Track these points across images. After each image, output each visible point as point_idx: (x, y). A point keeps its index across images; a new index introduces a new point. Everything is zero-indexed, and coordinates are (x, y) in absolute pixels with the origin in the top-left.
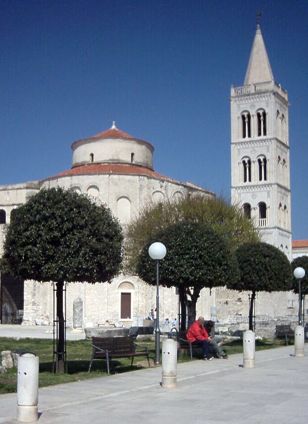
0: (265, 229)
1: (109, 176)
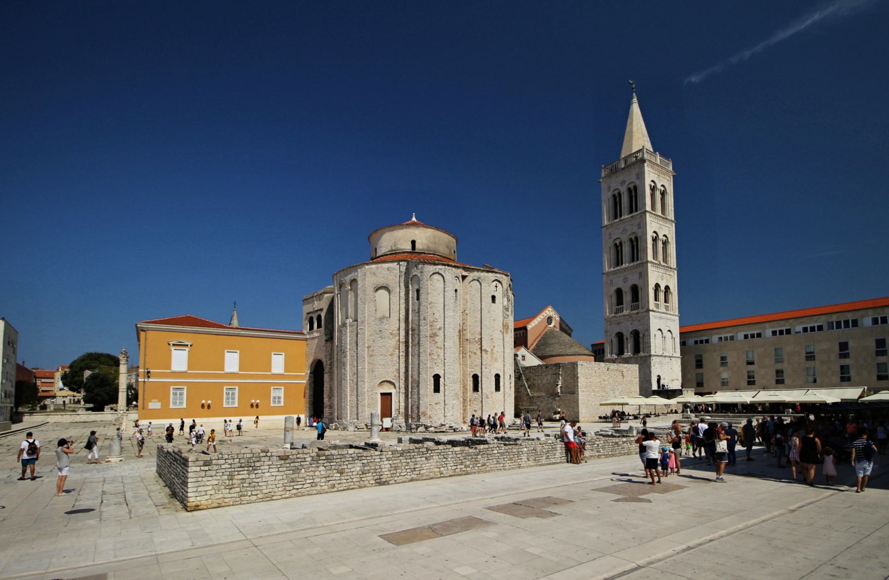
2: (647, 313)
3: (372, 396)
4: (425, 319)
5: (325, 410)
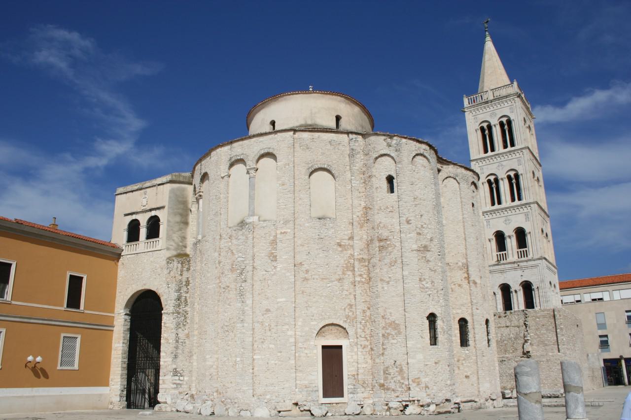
0: (527, 261)
1: (294, 134)
2: (541, 260)
3: (306, 351)
4: (408, 222)
5: (160, 378)
